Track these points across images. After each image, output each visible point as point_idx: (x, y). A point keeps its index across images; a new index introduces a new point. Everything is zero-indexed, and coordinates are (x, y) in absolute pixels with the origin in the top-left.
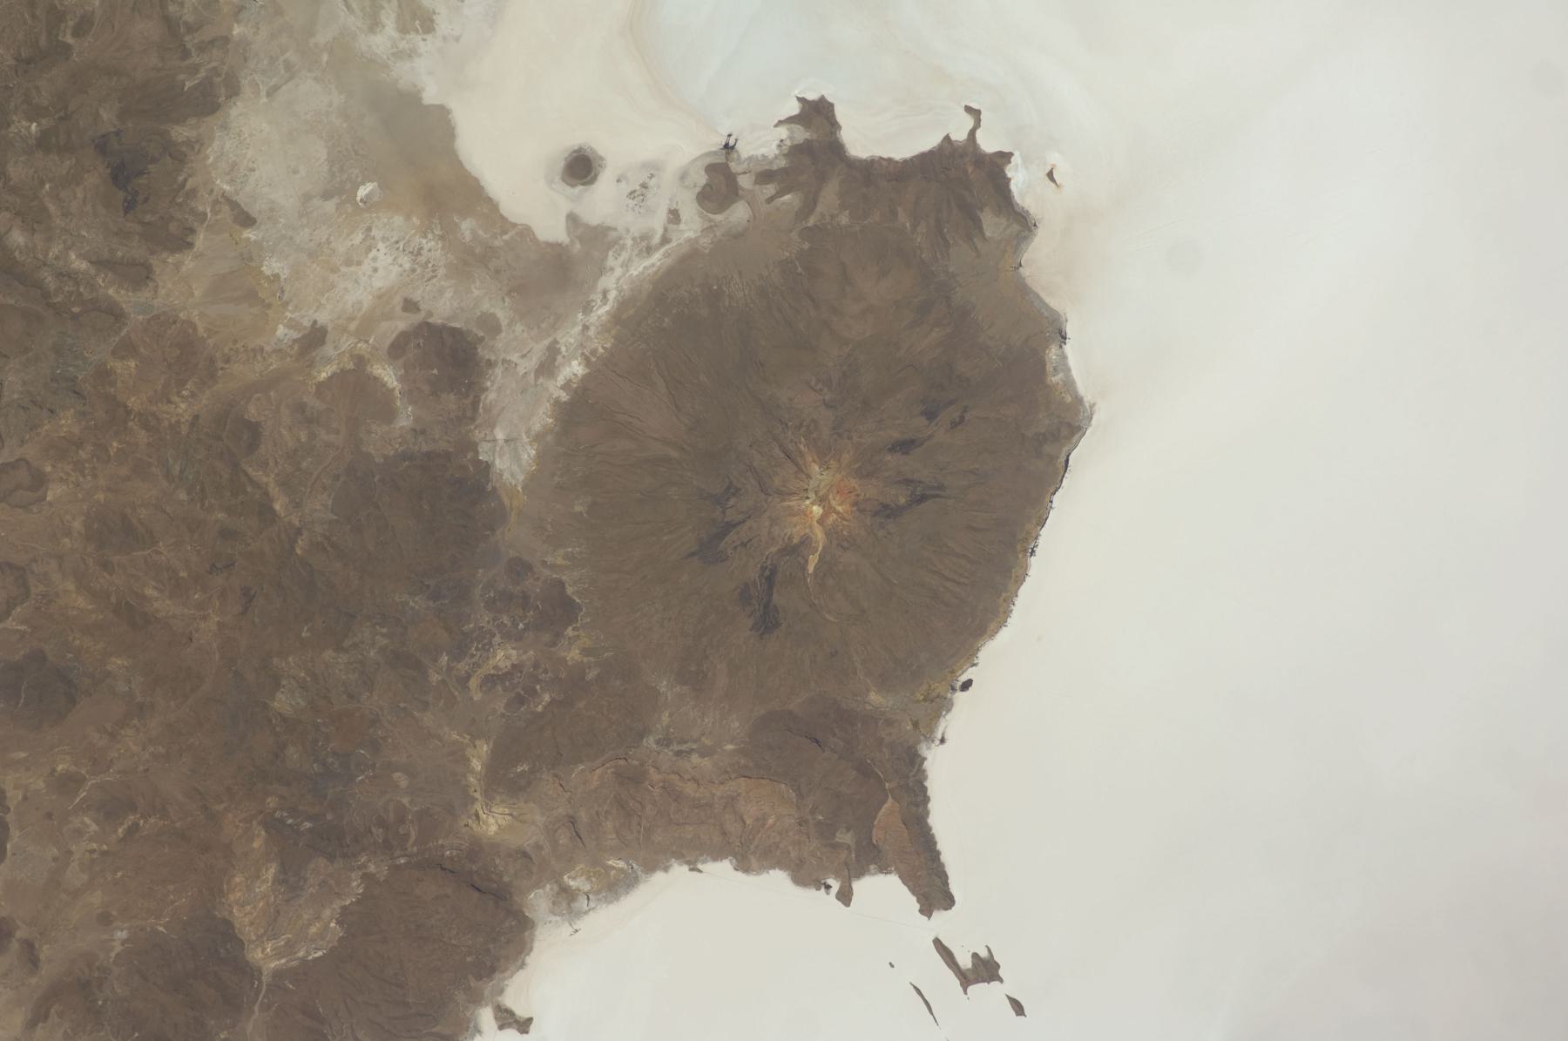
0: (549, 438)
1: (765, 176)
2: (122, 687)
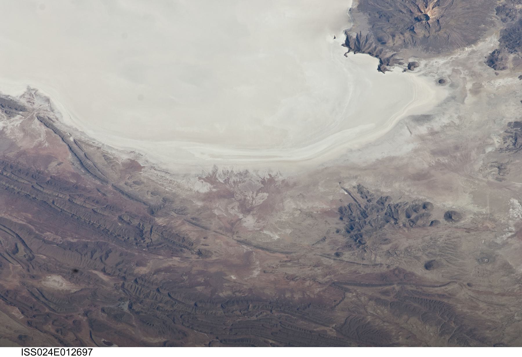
0: (481, 40)
1: (400, 64)
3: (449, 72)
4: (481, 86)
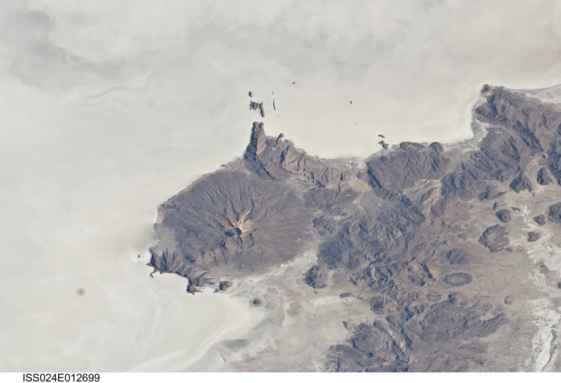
1: (211, 283)
3: (264, 291)
4: (299, 306)
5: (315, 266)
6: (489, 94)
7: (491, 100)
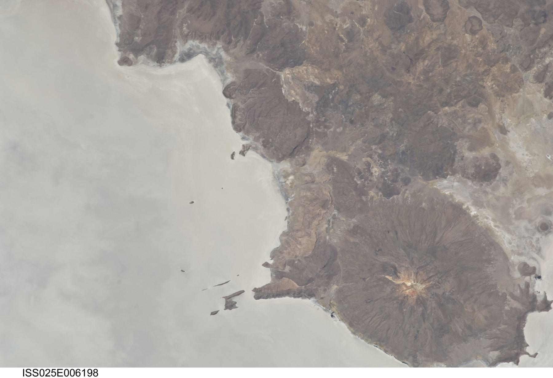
0: (451, 199)
2: (393, 46)
5: (463, 176)
6: (131, 56)
7: (138, 50)
